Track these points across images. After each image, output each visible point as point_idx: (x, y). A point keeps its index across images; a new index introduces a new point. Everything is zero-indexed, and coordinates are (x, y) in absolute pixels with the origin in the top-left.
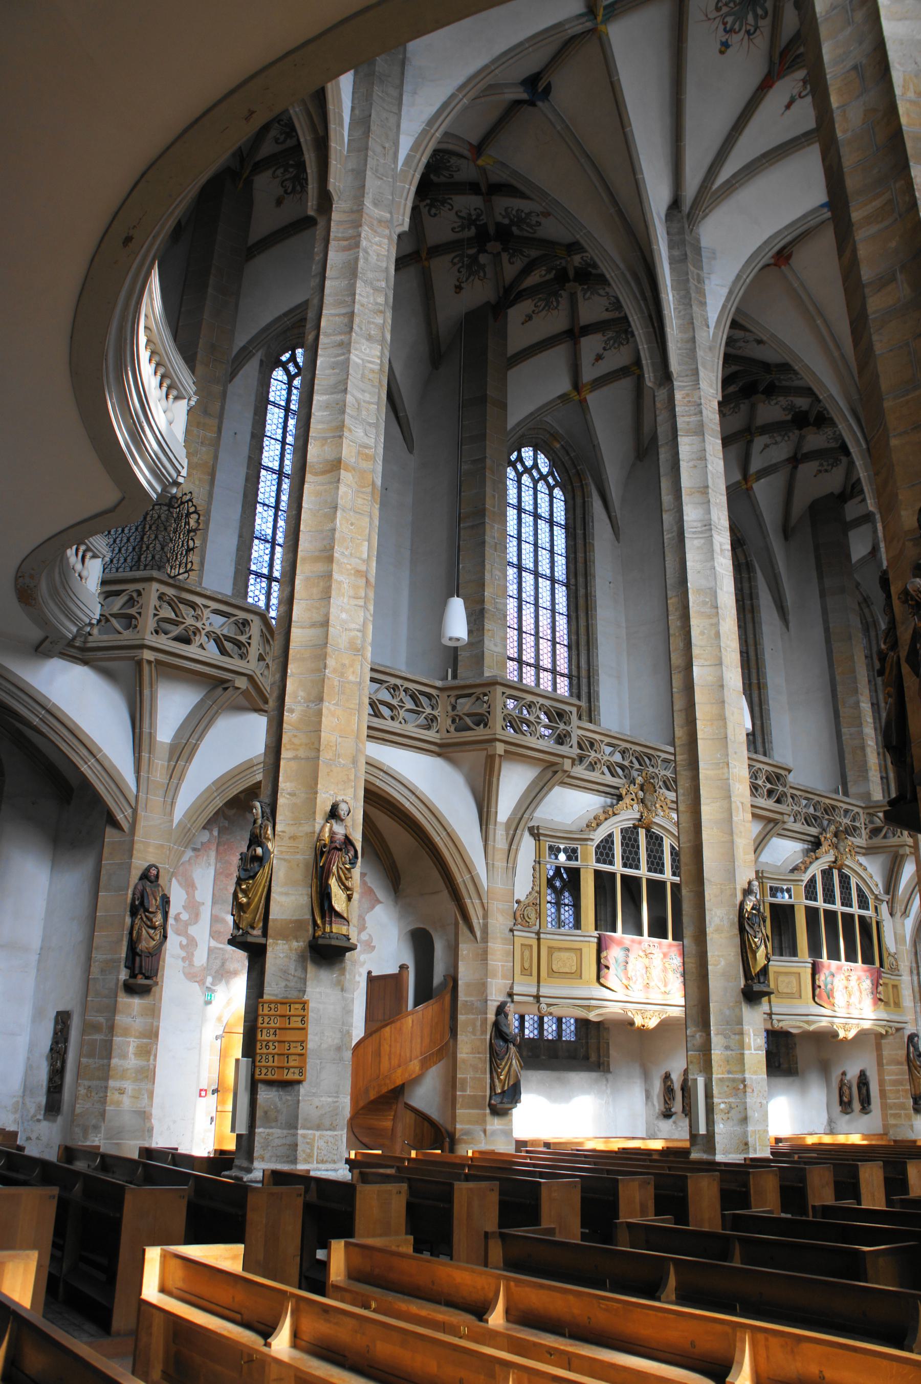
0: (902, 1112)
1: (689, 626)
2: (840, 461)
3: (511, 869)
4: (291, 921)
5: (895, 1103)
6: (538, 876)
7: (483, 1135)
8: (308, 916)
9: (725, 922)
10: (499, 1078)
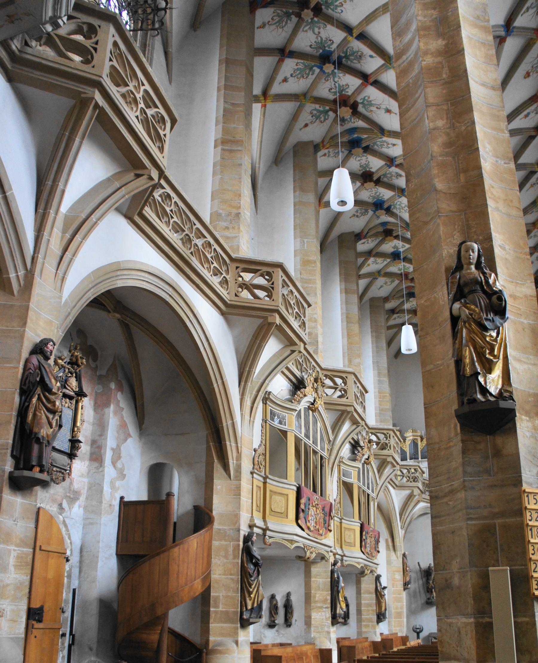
0: (370, 623)
2: (368, 212)
3: (251, 422)
4: (529, 395)
6: (264, 432)
7: (235, 646)
10: (250, 596)
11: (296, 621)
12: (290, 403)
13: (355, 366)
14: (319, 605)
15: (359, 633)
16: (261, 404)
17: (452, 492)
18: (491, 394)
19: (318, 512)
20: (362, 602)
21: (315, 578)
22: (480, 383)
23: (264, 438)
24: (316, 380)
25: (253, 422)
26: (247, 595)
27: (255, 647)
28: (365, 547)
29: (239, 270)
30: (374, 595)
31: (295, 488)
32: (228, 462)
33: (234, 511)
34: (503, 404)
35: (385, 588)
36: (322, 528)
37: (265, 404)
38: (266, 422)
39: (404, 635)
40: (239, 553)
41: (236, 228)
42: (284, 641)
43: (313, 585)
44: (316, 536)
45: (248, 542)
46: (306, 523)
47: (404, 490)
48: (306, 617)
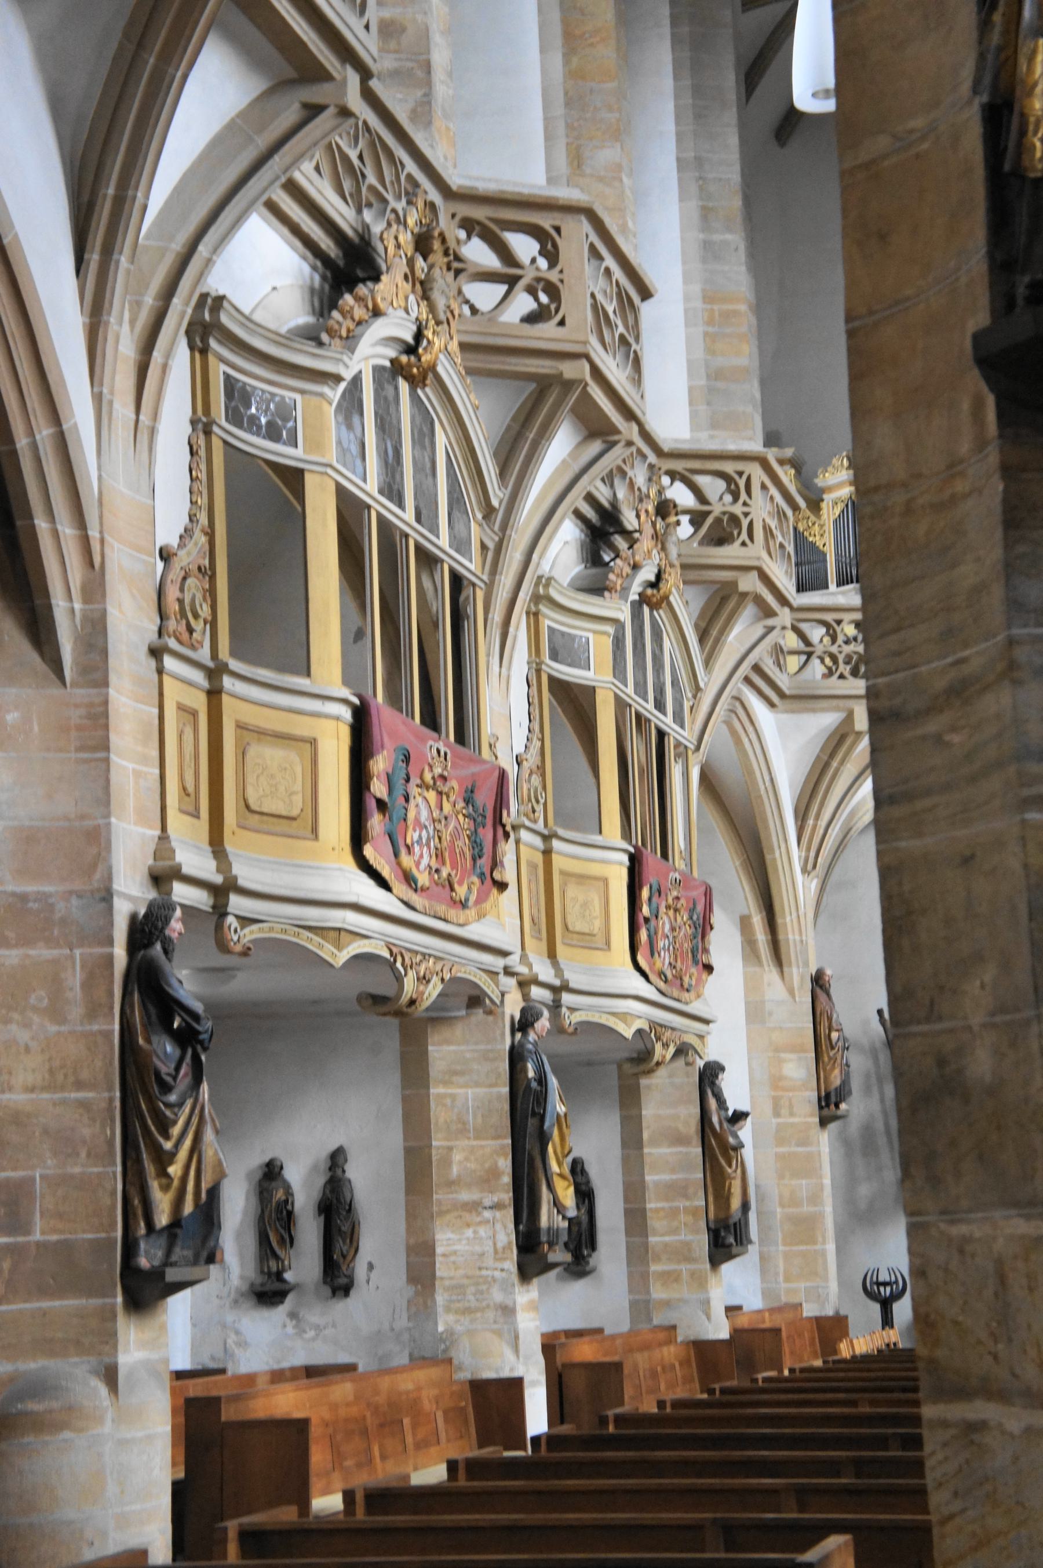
0: (684, 1268)
5: (666, 1245)
6: (203, 476)
7: (103, 1390)
10: (163, 1173)
11: (371, 1267)
12: (310, 347)
13: (601, 179)
15: (641, 1308)
19: (447, 807)
20: (648, 1178)
21: (446, 1083)
24: (423, 244)
25: (153, 432)
26: (150, 1168)
27: (195, 1388)
28: (652, 950)
30: (696, 1151)
31: (347, 714)
32: (49, 607)
33: (83, 817)
35: (739, 1117)
37: (199, 349)
38: (208, 433)
39: (830, 1312)
40: (111, 994)
42: (323, 1355)
43: (439, 1115)
44: (441, 909)
45: (150, 944)
46: (396, 854)
47: (814, 711)
48: (410, 1250)
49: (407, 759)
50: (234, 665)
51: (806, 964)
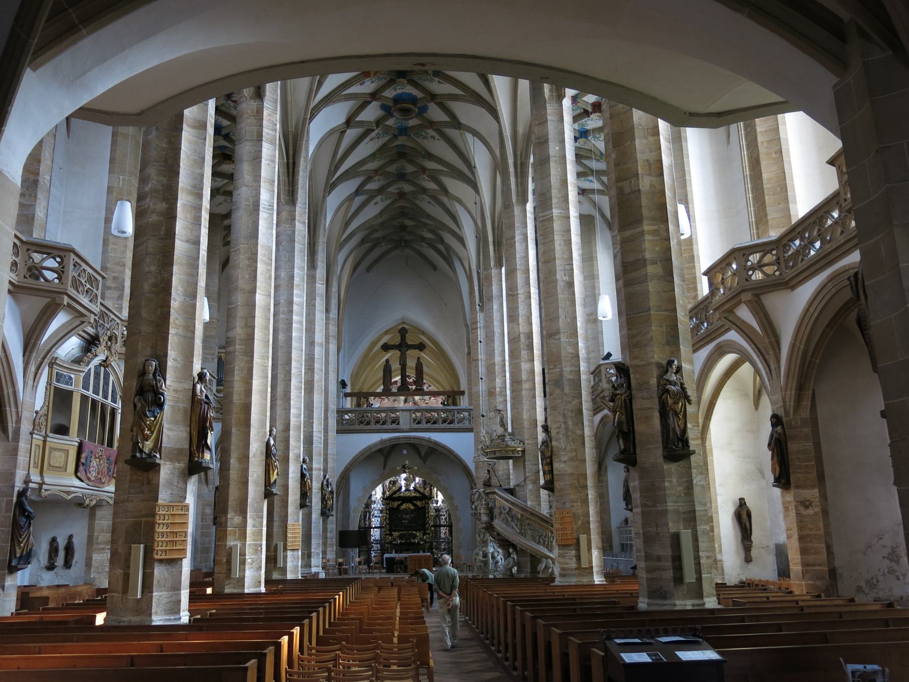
1: (256, 267)
3: (35, 387)
4: (175, 449)
6: (48, 394)
8: (187, 446)
9: (259, 452)
11: (76, 562)
12: (78, 365)
14: (101, 547)
16: (47, 368)
17: (124, 501)
18: (145, 453)
19: (102, 462)
21: (100, 520)
22: (139, 447)
23: (47, 400)
24: (110, 339)
25: (37, 387)
26: (16, 544)
27: (26, 590)
29: (29, 252)
31: (77, 444)
32: (8, 426)
33: (10, 470)
34: (149, 460)
36: (105, 476)
37: (51, 365)
38: (50, 385)
40: (11, 508)
41: (33, 195)
42: (62, 582)
43: (97, 527)
44: (97, 485)
45: (22, 497)
46: (86, 474)
48: (87, 559)
49: (92, 453)
50: (51, 435)
51: (214, 484)
